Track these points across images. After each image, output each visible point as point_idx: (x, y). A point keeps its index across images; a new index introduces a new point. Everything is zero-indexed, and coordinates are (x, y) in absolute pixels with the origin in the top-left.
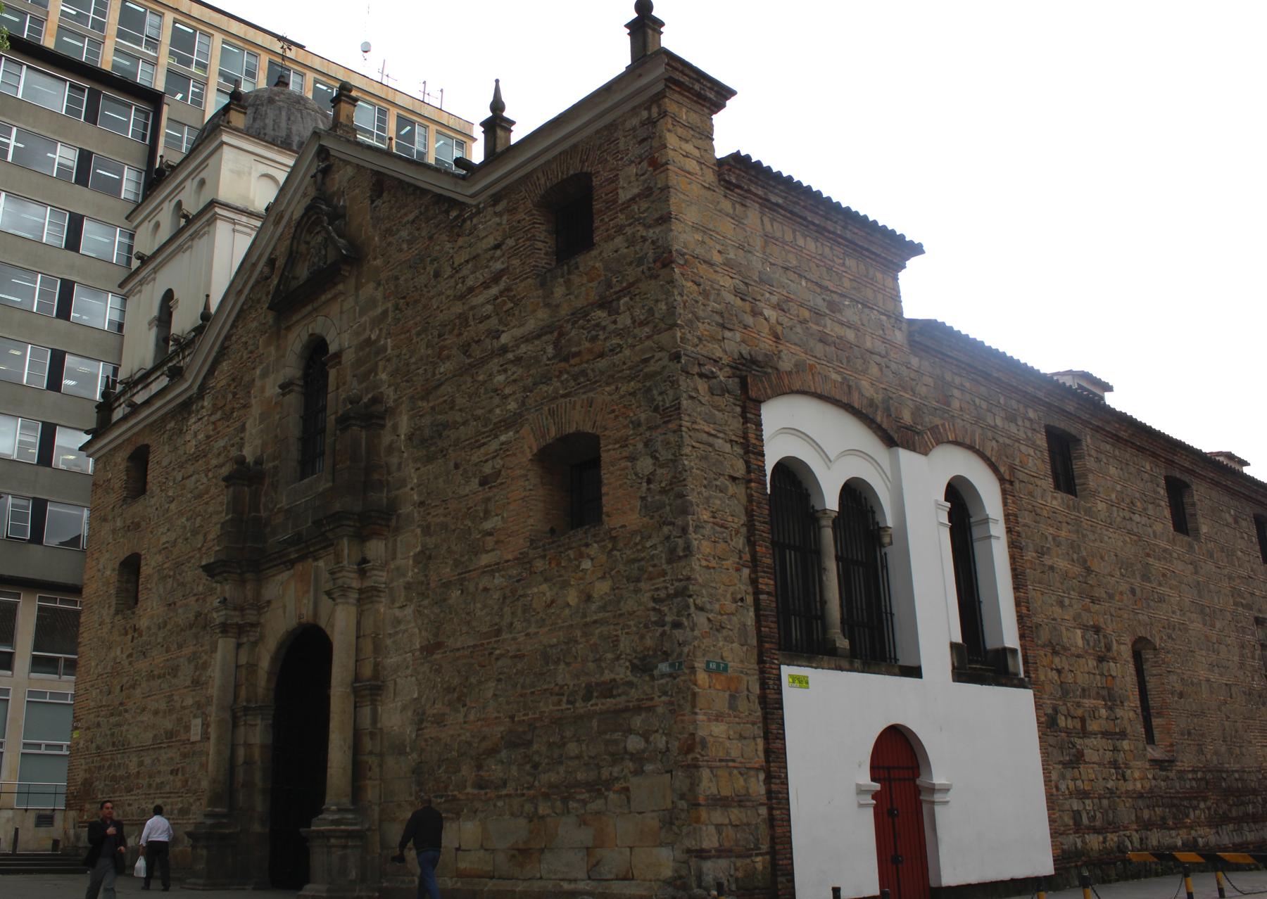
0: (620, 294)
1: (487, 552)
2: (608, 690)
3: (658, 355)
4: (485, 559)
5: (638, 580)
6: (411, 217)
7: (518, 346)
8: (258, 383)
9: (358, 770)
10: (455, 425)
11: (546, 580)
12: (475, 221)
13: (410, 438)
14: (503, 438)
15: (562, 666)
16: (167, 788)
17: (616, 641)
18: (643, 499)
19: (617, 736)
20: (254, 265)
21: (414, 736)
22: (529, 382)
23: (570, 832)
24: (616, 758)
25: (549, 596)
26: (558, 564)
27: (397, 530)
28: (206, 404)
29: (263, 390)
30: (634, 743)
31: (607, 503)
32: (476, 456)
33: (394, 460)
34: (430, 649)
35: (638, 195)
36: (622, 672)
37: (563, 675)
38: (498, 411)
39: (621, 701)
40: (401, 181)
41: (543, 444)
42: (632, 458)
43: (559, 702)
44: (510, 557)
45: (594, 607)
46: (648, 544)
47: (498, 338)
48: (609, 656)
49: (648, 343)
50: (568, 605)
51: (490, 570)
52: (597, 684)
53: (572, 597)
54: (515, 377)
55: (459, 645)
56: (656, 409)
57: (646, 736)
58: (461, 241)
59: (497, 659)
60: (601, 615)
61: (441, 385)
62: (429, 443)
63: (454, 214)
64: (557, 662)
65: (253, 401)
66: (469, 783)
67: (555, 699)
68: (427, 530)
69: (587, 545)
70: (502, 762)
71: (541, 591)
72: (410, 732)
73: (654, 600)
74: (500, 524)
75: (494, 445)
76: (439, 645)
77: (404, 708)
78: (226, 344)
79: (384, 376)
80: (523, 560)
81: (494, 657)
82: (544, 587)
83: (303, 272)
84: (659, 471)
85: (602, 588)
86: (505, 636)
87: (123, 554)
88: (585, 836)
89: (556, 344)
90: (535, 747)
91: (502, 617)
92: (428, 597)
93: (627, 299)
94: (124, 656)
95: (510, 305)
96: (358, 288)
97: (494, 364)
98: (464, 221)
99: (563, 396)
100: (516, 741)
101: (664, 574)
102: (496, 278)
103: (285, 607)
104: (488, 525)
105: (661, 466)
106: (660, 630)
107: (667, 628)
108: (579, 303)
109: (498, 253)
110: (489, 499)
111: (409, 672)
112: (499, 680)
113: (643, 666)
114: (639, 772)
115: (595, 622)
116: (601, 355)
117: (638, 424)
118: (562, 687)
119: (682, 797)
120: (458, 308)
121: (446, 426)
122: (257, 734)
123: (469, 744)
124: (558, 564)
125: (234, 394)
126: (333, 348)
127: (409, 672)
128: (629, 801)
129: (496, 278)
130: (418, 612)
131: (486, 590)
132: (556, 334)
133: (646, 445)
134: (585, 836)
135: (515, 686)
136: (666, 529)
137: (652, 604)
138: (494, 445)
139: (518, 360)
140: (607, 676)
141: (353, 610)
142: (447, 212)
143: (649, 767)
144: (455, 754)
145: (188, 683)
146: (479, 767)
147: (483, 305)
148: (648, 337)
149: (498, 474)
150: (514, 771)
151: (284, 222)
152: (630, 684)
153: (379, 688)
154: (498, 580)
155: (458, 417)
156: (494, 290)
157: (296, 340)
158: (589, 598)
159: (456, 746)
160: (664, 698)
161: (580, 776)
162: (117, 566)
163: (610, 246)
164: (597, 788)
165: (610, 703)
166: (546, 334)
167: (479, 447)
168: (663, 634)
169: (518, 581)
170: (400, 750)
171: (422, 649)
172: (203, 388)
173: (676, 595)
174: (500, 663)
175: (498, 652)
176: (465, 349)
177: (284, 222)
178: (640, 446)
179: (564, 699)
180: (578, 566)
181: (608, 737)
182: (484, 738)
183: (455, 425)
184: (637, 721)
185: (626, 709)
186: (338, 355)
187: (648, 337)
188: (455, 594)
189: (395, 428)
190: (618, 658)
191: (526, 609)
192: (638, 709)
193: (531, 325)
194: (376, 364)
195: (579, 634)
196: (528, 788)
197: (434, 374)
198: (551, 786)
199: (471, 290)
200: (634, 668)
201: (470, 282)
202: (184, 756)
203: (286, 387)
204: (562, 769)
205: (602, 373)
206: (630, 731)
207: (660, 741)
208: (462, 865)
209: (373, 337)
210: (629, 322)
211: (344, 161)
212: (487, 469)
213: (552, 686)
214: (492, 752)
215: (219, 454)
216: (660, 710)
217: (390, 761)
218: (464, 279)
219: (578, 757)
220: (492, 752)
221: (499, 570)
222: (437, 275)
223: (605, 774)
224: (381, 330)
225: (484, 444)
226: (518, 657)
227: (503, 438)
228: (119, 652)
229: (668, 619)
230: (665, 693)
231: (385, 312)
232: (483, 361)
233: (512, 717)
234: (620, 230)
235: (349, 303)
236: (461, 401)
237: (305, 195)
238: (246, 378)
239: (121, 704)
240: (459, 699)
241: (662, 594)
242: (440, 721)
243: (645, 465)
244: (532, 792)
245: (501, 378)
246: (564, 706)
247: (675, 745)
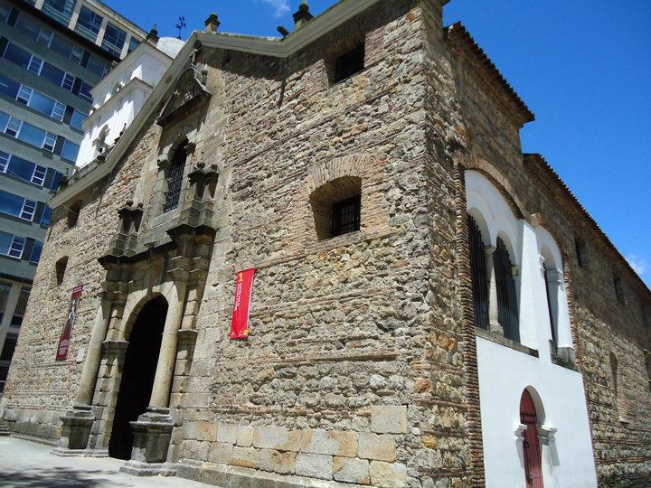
8: (146, 164)
19: (361, 375)
22: (314, 150)
23: (320, 440)
30: (376, 380)
31: (364, 219)
37: (324, 331)
39: (368, 351)
41: (320, 184)
44: (291, 254)
53: (334, 279)
57: (387, 375)
60: (355, 291)
62: (245, 190)
72: (212, 362)
87: (59, 257)
88: (331, 446)
105: (408, 194)
116: (366, 130)
134: (331, 446)
141: (185, 284)
151: (172, 81)
152: (376, 338)
160: (403, 350)
162: (55, 264)
163: (374, 70)
164: (346, 410)
168: (403, 306)
176: (272, 135)
177: (172, 81)
193: (318, 117)
196: (290, 407)
208: (237, 457)
223: (353, 399)
241: (405, 278)
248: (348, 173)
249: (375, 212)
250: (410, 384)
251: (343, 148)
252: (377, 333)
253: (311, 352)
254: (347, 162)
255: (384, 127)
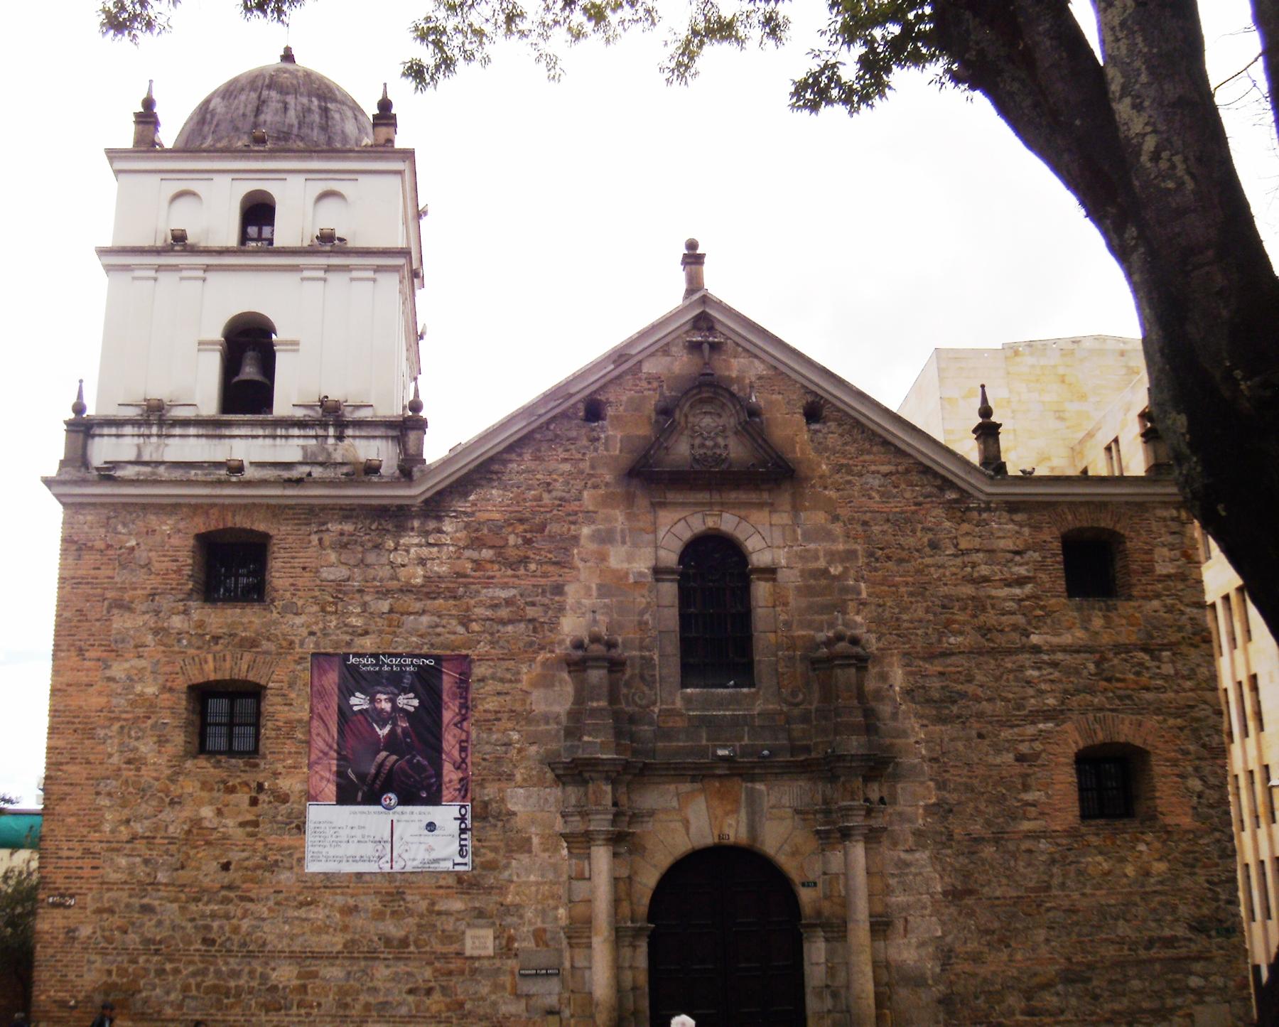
0: (1164, 647)
1: (1029, 820)
2: (1170, 942)
3: (1204, 706)
4: (1026, 826)
5: (1193, 866)
6: (885, 469)
7: (1053, 652)
9: (880, 1000)
10: (977, 699)
11: (1101, 853)
12: (985, 515)
13: (908, 693)
14: (1041, 726)
15: (1121, 922)
16: (404, 1010)
17: (1174, 909)
18: (1194, 808)
19: (1178, 976)
20: (571, 395)
21: (938, 970)
24: (1177, 992)
25: (1106, 866)
26: (1114, 843)
27: (896, 777)
28: (448, 526)
29: (603, 558)
30: (1194, 982)
32: (1006, 734)
33: (885, 709)
34: (954, 895)
35: (1175, 575)
36: (1181, 931)
37: (1123, 929)
38: (1033, 701)
39: (1183, 952)
40: (858, 422)
41: (1090, 742)
42: (1182, 776)
43: (1121, 950)
44: (1058, 828)
45: (1152, 880)
46: (1201, 842)
47: (1028, 636)
48: (1169, 918)
49: (1190, 694)
50: (1126, 876)
51: (1034, 836)
52: (1159, 938)
53: (1130, 870)
54: (1051, 677)
55: (998, 893)
56: (1204, 746)
57: (1205, 976)
58: (966, 527)
59: (1048, 910)
60: (1159, 887)
61: (952, 654)
63: (951, 495)
64: (1116, 919)
65: (580, 565)
66: (1017, 1012)
67: (1117, 947)
68: (942, 786)
69: (1142, 833)
70: (1058, 994)
71: (1097, 863)
72: (931, 967)
73: (1208, 882)
74: (1044, 799)
75: (1030, 730)
76: (970, 892)
77: (922, 944)
78: (496, 467)
79: (859, 619)
80: (1072, 833)
81: (1042, 910)
82: (1099, 858)
83: (682, 450)
84: (1207, 791)
85: (1160, 867)
86: (1055, 892)
89: (1097, 664)
90: (1095, 983)
91: (1052, 876)
92: (951, 847)
93: (1168, 653)
94: (230, 822)
95: (1039, 612)
96: (796, 509)
97: (1025, 658)
98: (968, 509)
99: (1112, 710)
100: (1070, 977)
101: (1217, 865)
102: (1021, 582)
103: (686, 824)
104: (1029, 797)
105: (1208, 788)
106: (1215, 904)
107: (1222, 904)
108: (1122, 639)
109: (1017, 558)
110: (1028, 775)
111: (927, 912)
112: (1053, 928)
113: (1199, 927)
114: (1201, 1002)
115: (1155, 892)
116: (1148, 689)
117: (1186, 753)
118: (1123, 938)
119: (1240, 1019)
120: (969, 590)
121: (963, 695)
122: (641, 957)
123: (1018, 979)
124: (1114, 843)
125: (528, 542)
126: (760, 556)
127: (927, 912)
128: (1193, 1021)
129: (1021, 582)
130: (935, 858)
131: (1030, 851)
132: (1097, 656)
133: (1197, 769)
135: (1068, 934)
136: (1217, 835)
137: (1206, 885)
138: (1030, 730)
139: (1054, 665)
140: (1167, 932)
142: (941, 489)
143: (1209, 999)
144: (998, 987)
145: (451, 881)
146: (1029, 999)
147: (1005, 600)
148: (1192, 690)
149: (1037, 756)
150: (1073, 1001)
152: (1190, 940)
153: (888, 924)
154: (1043, 845)
155: (979, 691)
156: (1017, 591)
157: (676, 527)
158: (1147, 874)
159: (1000, 980)
160: (1221, 952)
161: (1145, 1005)
162: (181, 683)
165: (1170, 953)
166: (1085, 652)
167: (1012, 727)
168: (1218, 908)
169: (1069, 850)
170: (917, 981)
171: (945, 893)
172: (435, 506)
173: (1227, 881)
174: (1051, 914)
175: (1048, 905)
178: (1190, 769)
179: (1126, 947)
180: (1134, 848)
181: (1170, 977)
182: (1035, 974)
183: (977, 699)
184: (1198, 967)
185: (1188, 958)
186: (770, 572)
187: (1192, 690)
188: (988, 851)
189: (884, 677)
190: (1177, 920)
191: (1080, 873)
192: (1198, 958)
193: (1067, 639)
194: (845, 601)
195: (1138, 899)
197: (940, 641)
198: (1114, 1012)
199: (986, 579)
200: (1191, 928)
201: (984, 570)
202: (450, 973)
203: (659, 572)
204: (1125, 1001)
205: (1149, 703)
206: (1191, 973)
207: (1220, 981)
209: (832, 570)
210: (1172, 672)
211: (747, 351)
212: (1024, 748)
213: (1113, 936)
214: (1047, 986)
215: (495, 607)
216: (1218, 960)
217: (903, 993)
218: (974, 565)
219: (1142, 992)
220: (1047, 986)
221: (1045, 838)
222: (934, 546)
223: (1169, 1002)
224: (846, 569)
225: (1018, 726)
226: (1072, 911)
227: (1041, 726)
228: (207, 812)
229: (1223, 897)
230: (1221, 948)
231: (850, 555)
232: (1010, 652)
233: (1069, 959)
234: (1158, 596)
235: (783, 518)
236: (980, 677)
237: (665, 350)
238: (554, 528)
239: (230, 887)
240: (1000, 941)
241: (1216, 879)
242: (976, 958)
243: (1196, 784)
244: (1094, 1018)
245: (1036, 673)
246: (1126, 952)
247: (1231, 984)
248: (1130, 739)
249: (1174, 799)
250: (1231, 984)
251: (1117, 702)
252: (1189, 935)
253: (1110, 952)
254: (1127, 722)
255: (1172, 695)
